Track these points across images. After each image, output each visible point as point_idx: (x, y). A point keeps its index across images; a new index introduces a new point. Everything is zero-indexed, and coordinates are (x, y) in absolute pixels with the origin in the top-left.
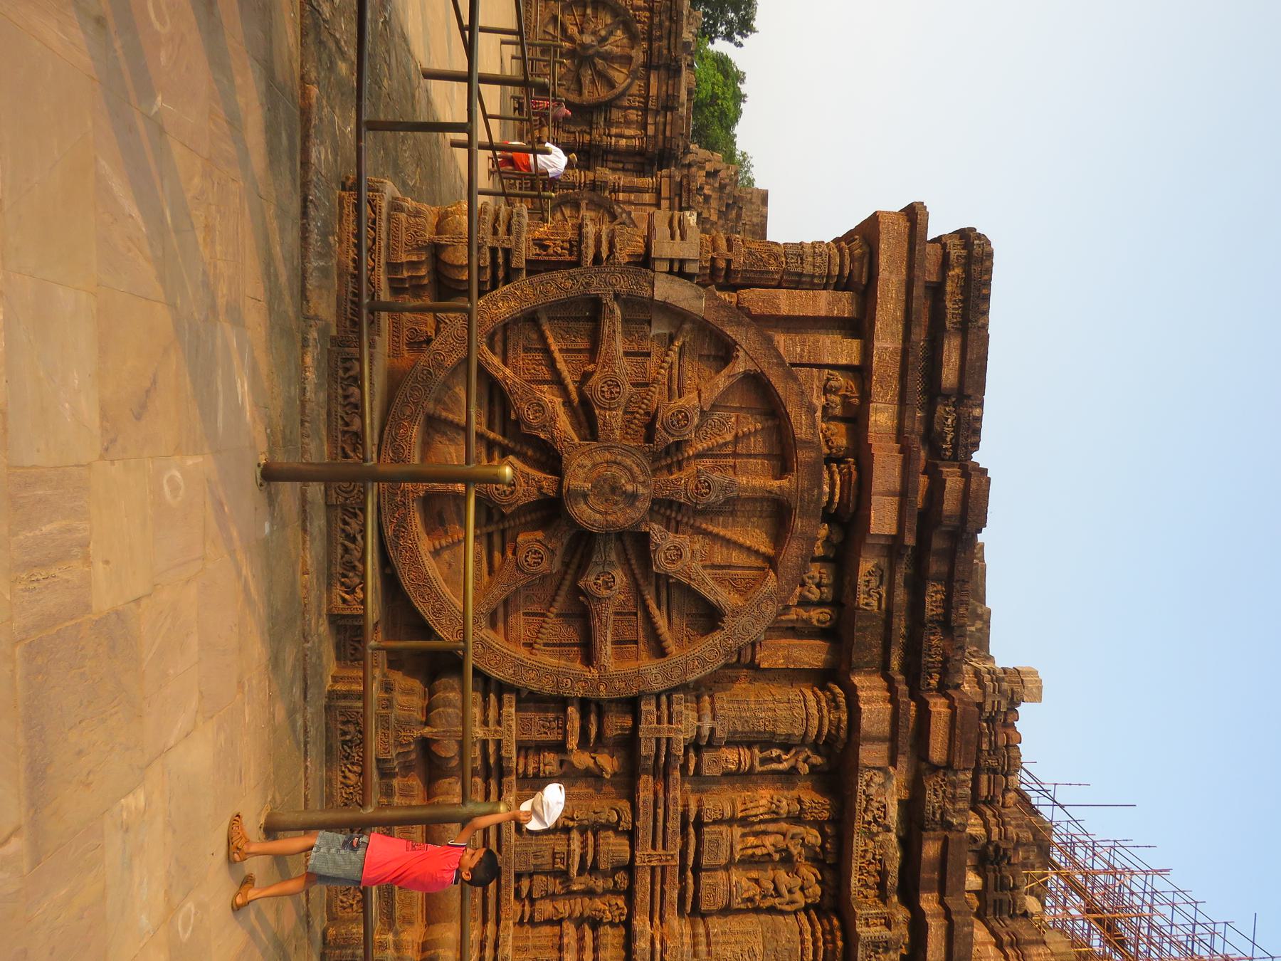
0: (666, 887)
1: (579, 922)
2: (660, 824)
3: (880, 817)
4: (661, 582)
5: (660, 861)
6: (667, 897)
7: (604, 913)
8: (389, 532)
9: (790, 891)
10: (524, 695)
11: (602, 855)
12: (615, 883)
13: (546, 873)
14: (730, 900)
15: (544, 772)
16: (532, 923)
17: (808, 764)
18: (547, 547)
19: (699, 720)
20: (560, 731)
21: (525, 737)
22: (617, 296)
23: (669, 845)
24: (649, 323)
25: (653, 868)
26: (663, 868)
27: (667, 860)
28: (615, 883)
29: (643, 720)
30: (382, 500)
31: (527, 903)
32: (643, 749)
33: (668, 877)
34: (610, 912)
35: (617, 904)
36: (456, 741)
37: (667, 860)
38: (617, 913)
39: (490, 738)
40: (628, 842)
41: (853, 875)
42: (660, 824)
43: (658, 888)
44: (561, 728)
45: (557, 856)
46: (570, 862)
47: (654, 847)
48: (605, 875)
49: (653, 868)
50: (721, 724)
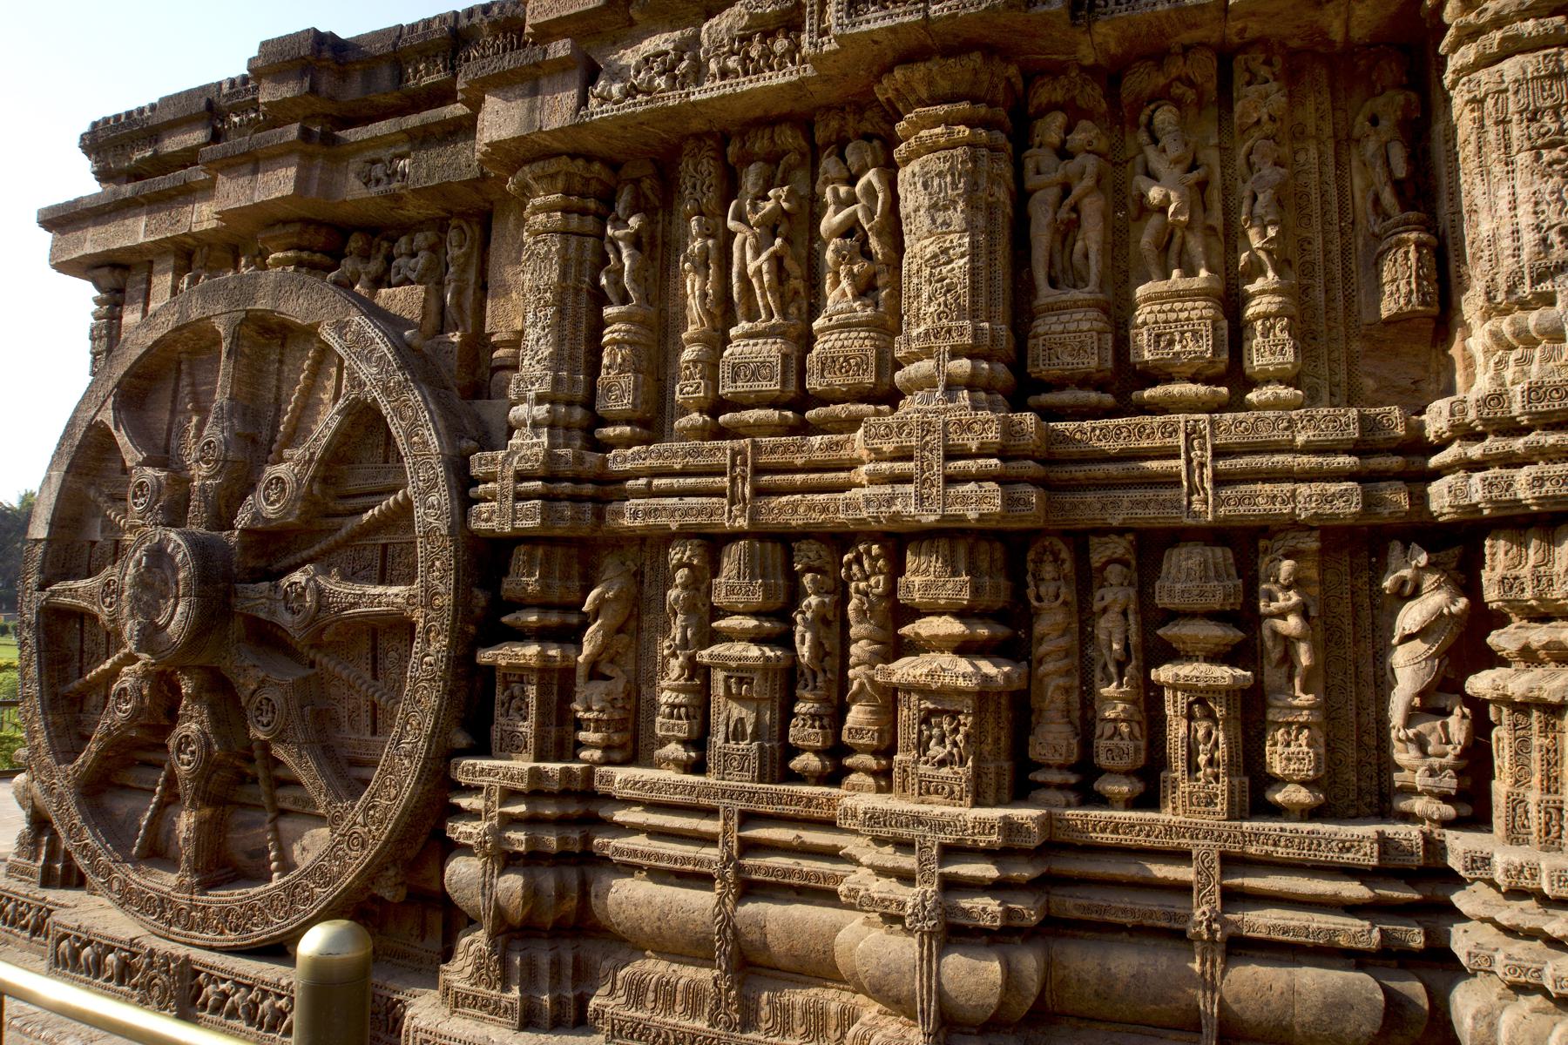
0: (799, 462)
1: (899, 648)
2: (677, 482)
3: (664, 63)
4: (340, 508)
6: (818, 456)
7: (866, 594)
8: (231, 938)
9: (852, 200)
10: (461, 740)
11: (733, 598)
13: (787, 715)
14: (859, 324)
16: (887, 750)
17: (629, 216)
18: (255, 691)
22: (42, 588)
24: (94, 543)
25: (759, 492)
26: (759, 470)
27: (744, 463)
28: (809, 569)
30: (197, 942)
31: (848, 762)
32: (528, 524)
34: (867, 578)
35: (849, 565)
36: (501, 874)
37: (744, 463)
39: (498, 810)
41: (768, 83)
42: (677, 482)
43: (799, 478)
46: (734, 664)
47: (720, 493)
48: (795, 595)
49: (759, 492)
50: (533, 384)
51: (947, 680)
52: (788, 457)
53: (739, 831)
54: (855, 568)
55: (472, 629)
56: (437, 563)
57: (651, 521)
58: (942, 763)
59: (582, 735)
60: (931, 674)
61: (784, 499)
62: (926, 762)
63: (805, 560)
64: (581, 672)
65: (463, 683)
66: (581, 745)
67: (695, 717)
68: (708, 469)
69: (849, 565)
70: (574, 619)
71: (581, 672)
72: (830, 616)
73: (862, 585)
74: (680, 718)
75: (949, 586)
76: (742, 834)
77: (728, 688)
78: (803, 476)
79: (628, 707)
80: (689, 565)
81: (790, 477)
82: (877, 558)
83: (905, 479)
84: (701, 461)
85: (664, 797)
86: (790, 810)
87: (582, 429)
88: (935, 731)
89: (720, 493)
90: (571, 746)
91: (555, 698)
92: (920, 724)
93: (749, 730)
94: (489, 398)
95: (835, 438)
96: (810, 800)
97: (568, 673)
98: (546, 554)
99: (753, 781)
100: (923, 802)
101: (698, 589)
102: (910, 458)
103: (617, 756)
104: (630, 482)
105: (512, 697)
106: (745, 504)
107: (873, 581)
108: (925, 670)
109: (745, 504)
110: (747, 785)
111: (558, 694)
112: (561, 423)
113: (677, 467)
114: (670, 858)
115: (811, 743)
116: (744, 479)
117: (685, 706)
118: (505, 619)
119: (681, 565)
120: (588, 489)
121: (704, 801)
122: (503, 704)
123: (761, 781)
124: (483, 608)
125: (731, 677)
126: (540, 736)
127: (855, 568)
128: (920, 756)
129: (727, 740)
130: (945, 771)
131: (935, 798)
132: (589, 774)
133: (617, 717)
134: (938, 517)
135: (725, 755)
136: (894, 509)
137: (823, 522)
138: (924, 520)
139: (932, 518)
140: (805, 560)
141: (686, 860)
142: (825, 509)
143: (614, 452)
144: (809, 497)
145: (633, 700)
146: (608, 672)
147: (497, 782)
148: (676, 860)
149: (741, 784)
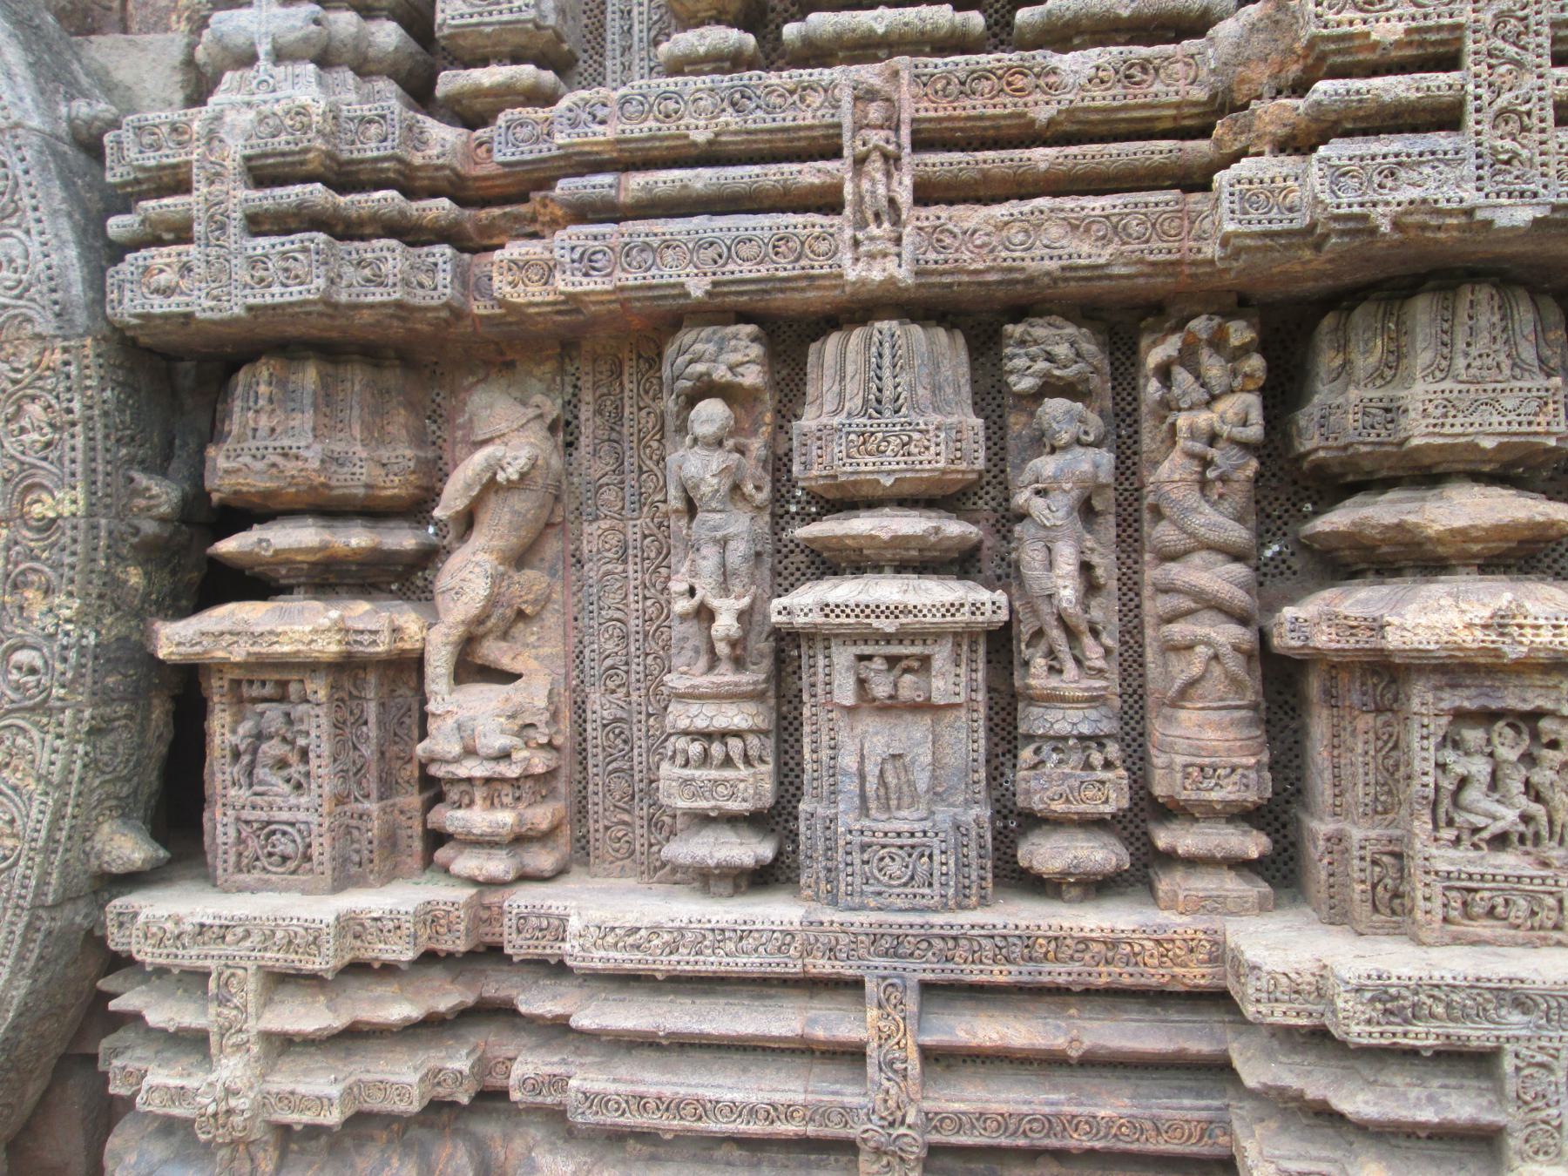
0: (1042, 112)
2: (701, 179)
5: (891, 161)
6: (1100, 98)
12: (1050, 388)
15: (505, 755)
19: (247, 59)
20: (293, 689)
21: (322, 849)
23: (808, 116)
28: (1050, 388)
29: (173, 305)
32: (295, 293)
33: (984, 106)
35: (1164, 373)
38: (1214, 368)
40: (833, 341)
42: (701, 179)
43: (1042, 157)
44: (283, 684)
45: (881, 690)
46: (888, 625)
51: (1546, 636)
52: (1006, 105)
53: (920, 1030)
54: (1182, 376)
55: (134, 577)
56: (35, 409)
57: (631, 279)
58: (1500, 841)
59: (451, 818)
60: (1499, 623)
61: (1000, 211)
62: (1457, 842)
63: (1041, 365)
64: (439, 664)
65: (123, 709)
66: (437, 838)
67: (762, 760)
68: (780, 141)
69: (1164, 373)
70: (403, 539)
71: (439, 664)
72: (1098, 504)
73: (1203, 419)
74: (728, 762)
75: (1509, 403)
76: (928, 1040)
77: (862, 683)
78: (1052, 152)
79: (558, 741)
80: (727, 392)
81: (1017, 154)
82: (1244, 351)
83: (1446, 117)
84: (758, 120)
85: (712, 963)
86: (1057, 973)
87: (394, 75)
88: (1479, 767)
89: (827, 201)
90: (418, 845)
91: (372, 730)
92: (1441, 745)
93: (922, 781)
94: (125, 30)
95: (1142, 51)
96: (1113, 944)
97: (409, 666)
98: (322, 376)
99: (946, 907)
100: (1456, 940)
101: (741, 450)
102: (1450, 62)
103: (543, 860)
104: (562, 183)
105: (260, 737)
106: (897, 222)
107: (1230, 406)
108: (1482, 613)
109: (897, 222)
110: (938, 919)
111: (381, 723)
112: (348, 56)
113: (700, 137)
114: (733, 1107)
115: (1082, 807)
116: (891, 161)
117: (738, 734)
118: (228, 546)
119: (707, 389)
120: (440, 208)
121: (822, 966)
122: (236, 755)
123: (961, 907)
124: (163, 520)
125: (869, 658)
126: (345, 832)
127: (1182, 376)
128: (1436, 827)
129: (864, 810)
130: (1510, 862)
131: (1482, 928)
132: (483, 915)
133: (540, 769)
134: (1540, 213)
135: (864, 847)
136: (1416, 193)
137: (1107, 265)
138: (1503, 219)
139: (1523, 215)
140: (1041, 365)
141: (774, 1112)
142: (1118, 230)
143: (502, 119)
144: (1069, 203)
145: (565, 725)
146: (507, 663)
147: (248, 958)
148: (753, 1111)
149: (916, 919)
